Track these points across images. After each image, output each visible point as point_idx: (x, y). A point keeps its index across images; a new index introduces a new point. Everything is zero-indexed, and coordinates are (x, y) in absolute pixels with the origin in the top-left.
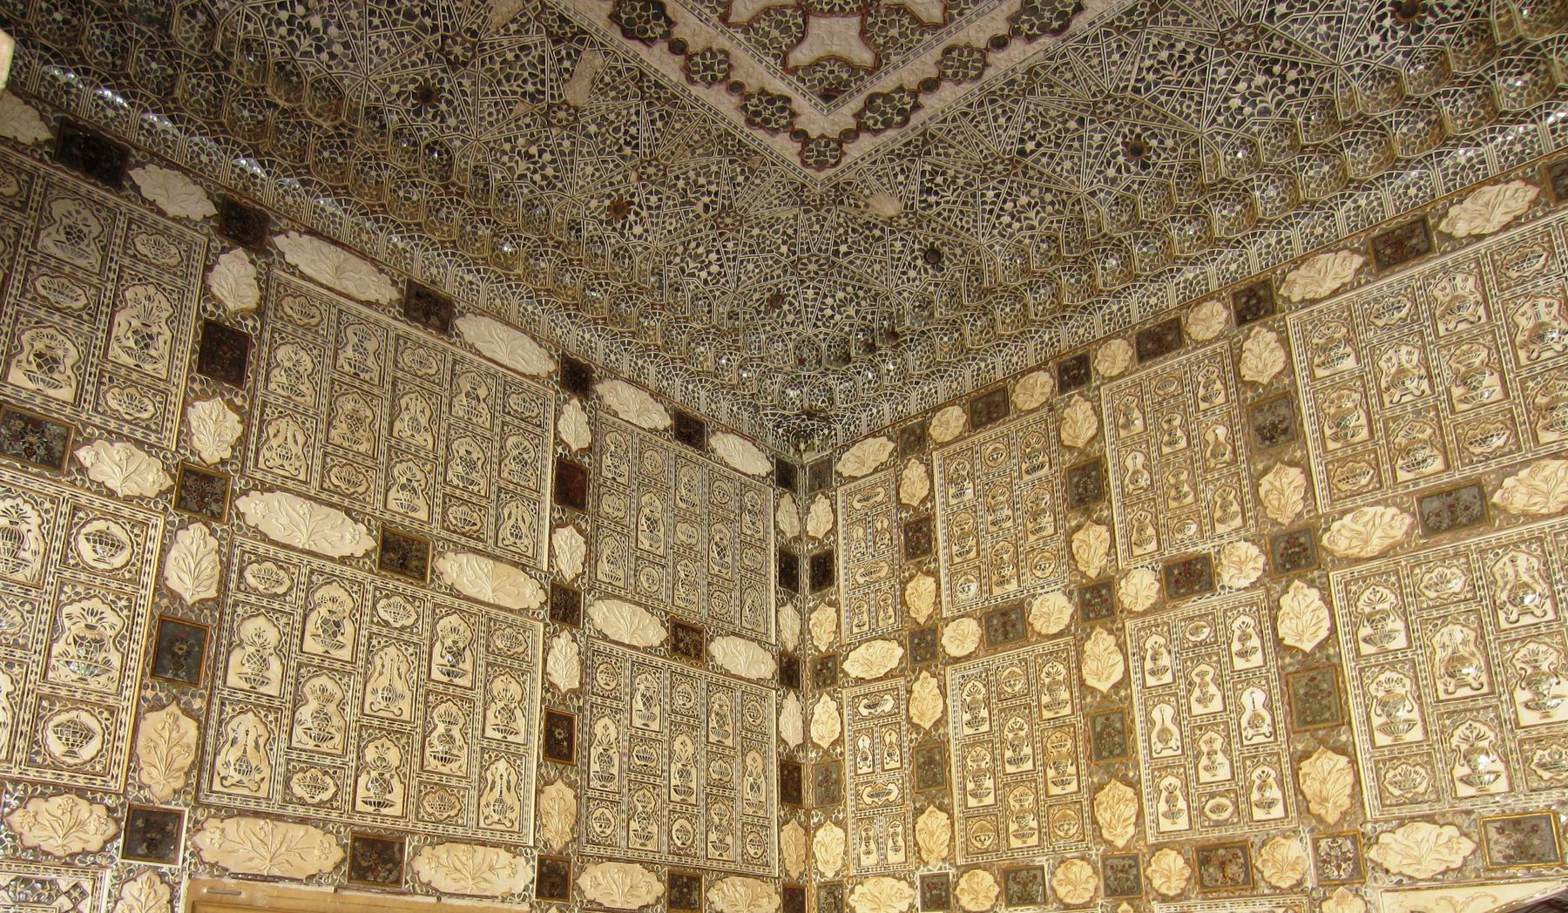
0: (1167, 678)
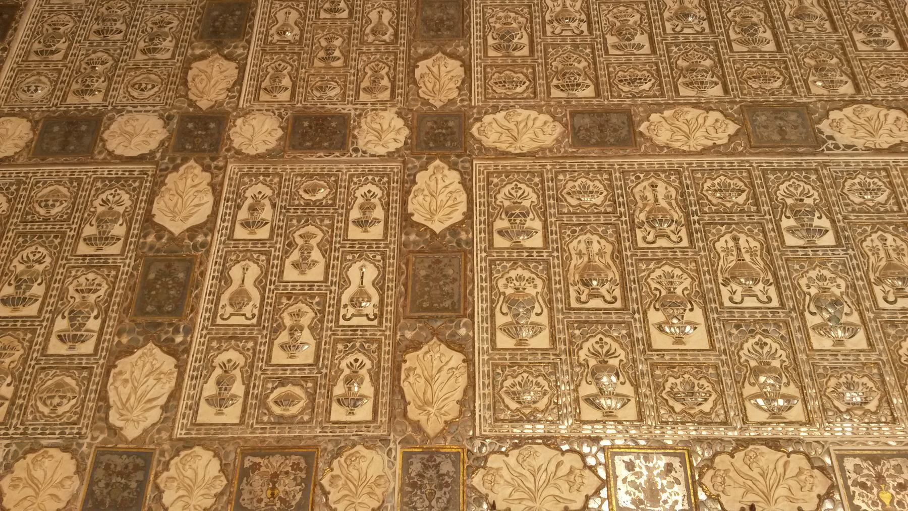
0: (263, 233)
